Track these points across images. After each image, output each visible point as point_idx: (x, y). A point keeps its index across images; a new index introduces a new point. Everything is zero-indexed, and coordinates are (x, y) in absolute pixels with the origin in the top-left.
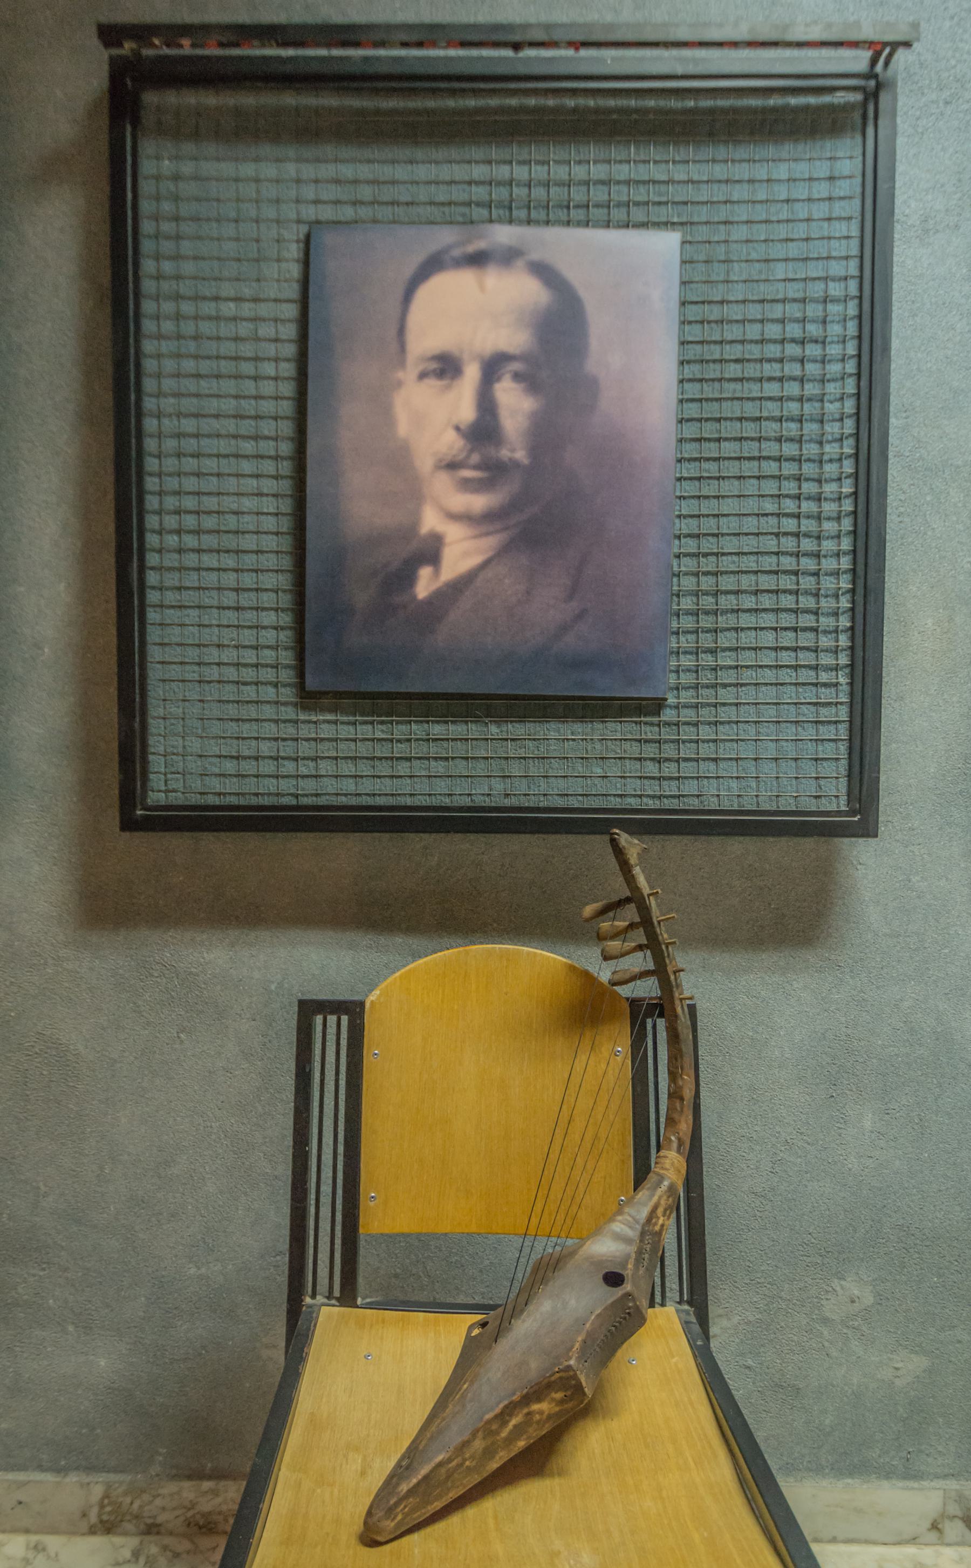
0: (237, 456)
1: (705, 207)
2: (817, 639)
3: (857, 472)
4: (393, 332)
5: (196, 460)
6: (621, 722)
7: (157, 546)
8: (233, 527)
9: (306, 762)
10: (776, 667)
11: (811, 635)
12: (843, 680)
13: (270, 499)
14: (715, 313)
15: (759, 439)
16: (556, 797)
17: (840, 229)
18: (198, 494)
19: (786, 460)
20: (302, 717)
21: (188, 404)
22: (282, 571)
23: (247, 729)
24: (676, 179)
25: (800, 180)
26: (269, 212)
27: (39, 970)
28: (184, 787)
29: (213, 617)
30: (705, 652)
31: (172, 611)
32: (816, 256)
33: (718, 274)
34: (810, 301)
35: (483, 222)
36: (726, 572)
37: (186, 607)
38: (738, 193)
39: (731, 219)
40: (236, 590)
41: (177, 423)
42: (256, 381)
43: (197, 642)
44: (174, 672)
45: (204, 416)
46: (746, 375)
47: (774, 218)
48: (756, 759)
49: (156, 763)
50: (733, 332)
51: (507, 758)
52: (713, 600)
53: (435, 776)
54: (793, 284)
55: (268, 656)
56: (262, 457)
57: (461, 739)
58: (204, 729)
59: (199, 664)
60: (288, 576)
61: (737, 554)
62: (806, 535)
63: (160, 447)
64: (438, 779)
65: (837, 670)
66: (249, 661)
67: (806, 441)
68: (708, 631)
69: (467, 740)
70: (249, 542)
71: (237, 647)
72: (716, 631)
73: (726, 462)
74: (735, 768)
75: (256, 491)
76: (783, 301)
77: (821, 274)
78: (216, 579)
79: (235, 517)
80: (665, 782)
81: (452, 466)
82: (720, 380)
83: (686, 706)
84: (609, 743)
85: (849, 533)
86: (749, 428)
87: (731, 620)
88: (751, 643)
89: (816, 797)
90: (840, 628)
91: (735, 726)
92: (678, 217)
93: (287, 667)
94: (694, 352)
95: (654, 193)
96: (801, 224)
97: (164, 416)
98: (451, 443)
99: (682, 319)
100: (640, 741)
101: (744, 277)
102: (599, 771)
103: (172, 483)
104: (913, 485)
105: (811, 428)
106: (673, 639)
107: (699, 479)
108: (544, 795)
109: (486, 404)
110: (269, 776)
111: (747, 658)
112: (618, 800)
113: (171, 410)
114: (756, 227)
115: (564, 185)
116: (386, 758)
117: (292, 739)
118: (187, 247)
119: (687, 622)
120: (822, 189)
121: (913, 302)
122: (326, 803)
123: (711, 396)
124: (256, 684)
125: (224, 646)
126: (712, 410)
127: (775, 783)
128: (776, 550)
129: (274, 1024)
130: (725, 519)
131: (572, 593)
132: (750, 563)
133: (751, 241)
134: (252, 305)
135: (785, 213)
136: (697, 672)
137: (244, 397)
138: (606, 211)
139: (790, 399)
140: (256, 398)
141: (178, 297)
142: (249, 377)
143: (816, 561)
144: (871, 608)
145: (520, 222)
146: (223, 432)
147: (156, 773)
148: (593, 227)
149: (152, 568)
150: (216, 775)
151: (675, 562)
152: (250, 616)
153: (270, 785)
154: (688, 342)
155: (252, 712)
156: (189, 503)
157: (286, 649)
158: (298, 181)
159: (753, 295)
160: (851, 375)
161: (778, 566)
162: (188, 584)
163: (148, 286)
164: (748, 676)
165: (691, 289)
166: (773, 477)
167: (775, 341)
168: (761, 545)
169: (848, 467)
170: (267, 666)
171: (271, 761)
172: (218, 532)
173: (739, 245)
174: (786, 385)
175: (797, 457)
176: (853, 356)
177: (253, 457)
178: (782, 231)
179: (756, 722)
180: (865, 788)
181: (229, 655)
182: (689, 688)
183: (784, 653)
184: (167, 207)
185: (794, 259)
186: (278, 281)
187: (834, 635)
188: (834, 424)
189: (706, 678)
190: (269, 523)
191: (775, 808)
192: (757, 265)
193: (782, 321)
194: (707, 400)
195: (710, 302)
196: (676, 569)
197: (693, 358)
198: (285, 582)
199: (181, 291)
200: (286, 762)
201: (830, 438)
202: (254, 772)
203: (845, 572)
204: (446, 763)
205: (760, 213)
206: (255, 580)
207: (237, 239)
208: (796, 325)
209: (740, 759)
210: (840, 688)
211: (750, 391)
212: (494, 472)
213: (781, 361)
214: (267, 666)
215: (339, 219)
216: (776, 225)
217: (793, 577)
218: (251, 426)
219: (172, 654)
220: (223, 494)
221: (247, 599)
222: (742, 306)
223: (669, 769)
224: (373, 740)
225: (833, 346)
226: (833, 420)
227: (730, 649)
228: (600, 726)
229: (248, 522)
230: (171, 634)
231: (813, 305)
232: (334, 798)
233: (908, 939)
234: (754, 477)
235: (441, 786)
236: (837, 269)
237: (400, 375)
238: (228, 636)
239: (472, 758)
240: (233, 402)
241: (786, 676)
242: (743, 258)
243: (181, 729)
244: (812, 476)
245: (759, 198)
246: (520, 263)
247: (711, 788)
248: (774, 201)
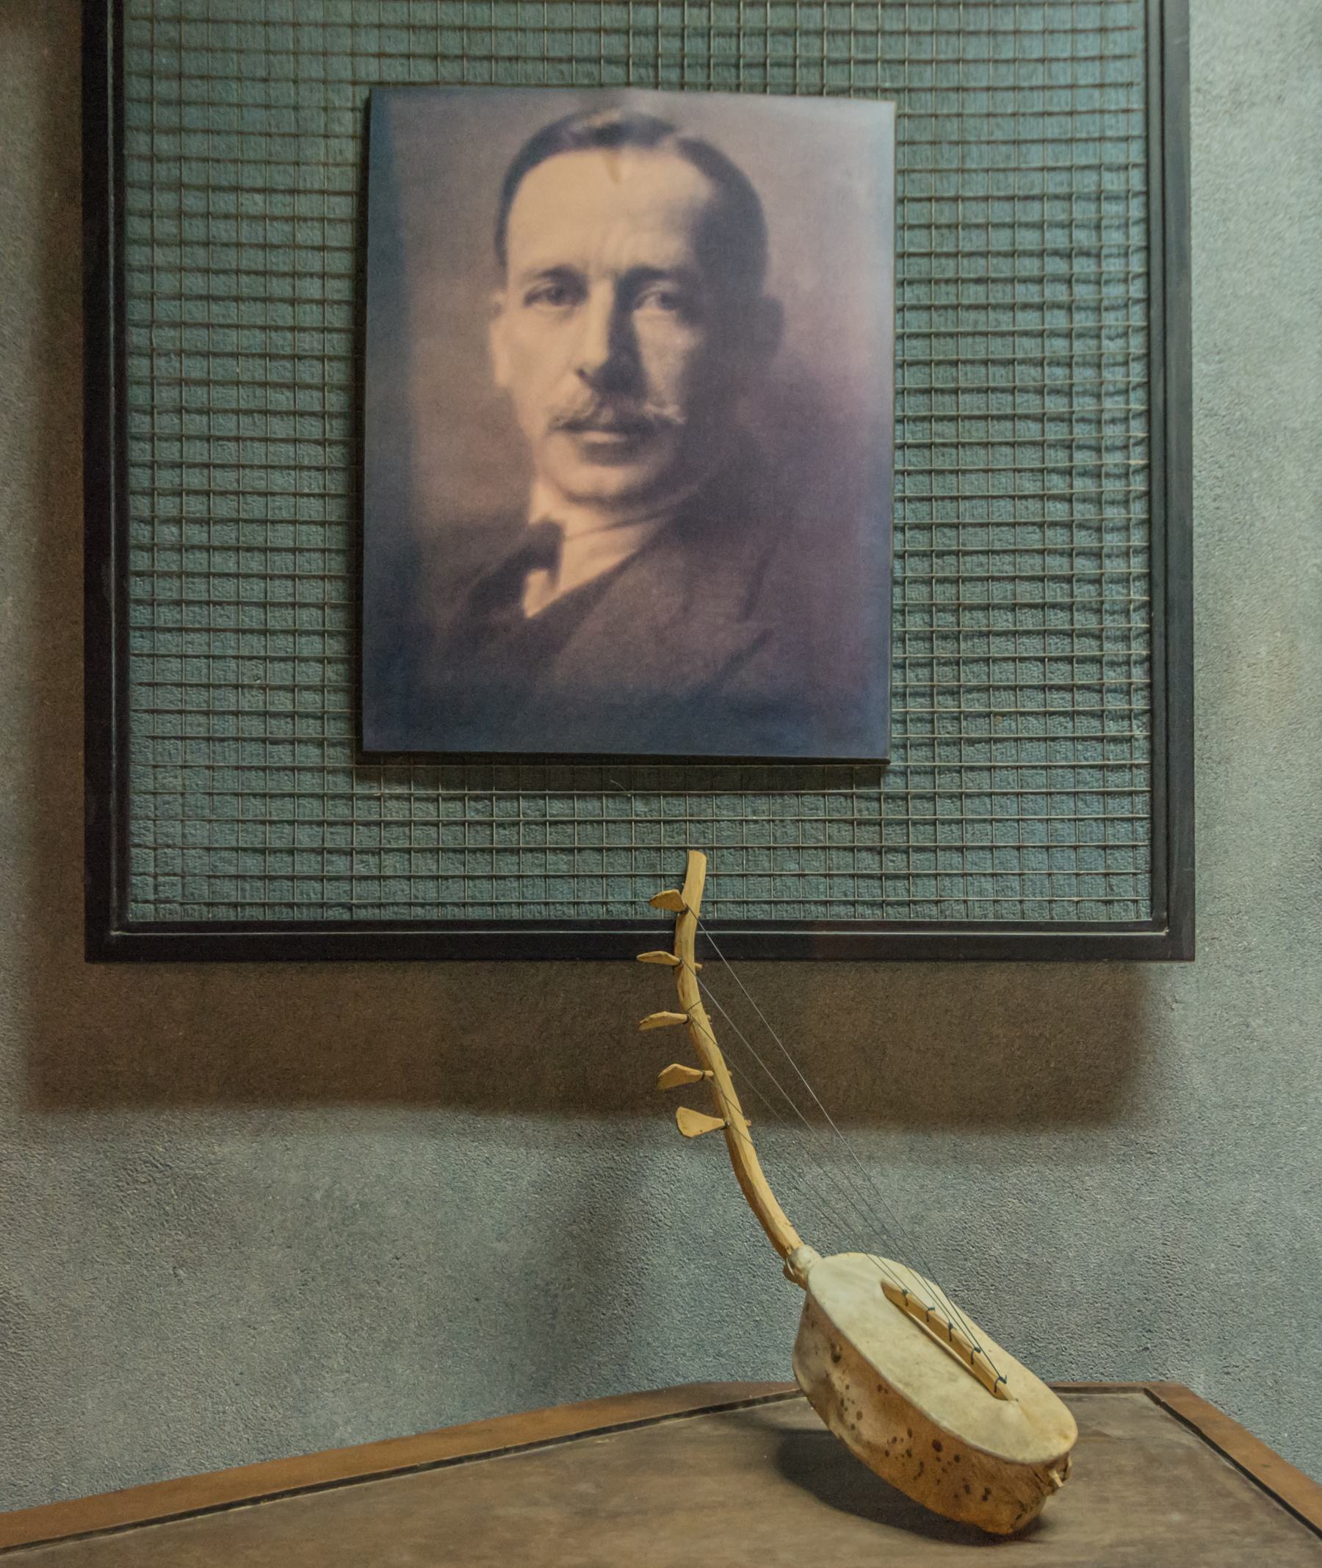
0: (265, 412)
1: (929, 68)
2: (1102, 673)
3: (1149, 438)
4: (488, 235)
5: (205, 418)
6: (824, 795)
7: (146, 541)
8: (258, 514)
9: (365, 857)
10: (1045, 714)
11: (1093, 668)
12: (1139, 732)
13: (313, 473)
14: (944, 214)
15: (1012, 391)
17: (1117, 99)
18: (207, 466)
19: (1051, 420)
20: (359, 790)
21: (196, 338)
22: (330, 578)
23: (278, 809)
24: (887, 28)
25: (1059, 32)
26: (313, 69)
28: (184, 895)
29: (229, 644)
30: (943, 694)
31: (168, 636)
32: (1084, 135)
33: (949, 161)
34: (1078, 198)
35: (617, 85)
36: (971, 579)
37: (187, 630)
38: (974, 49)
39: (965, 84)
40: (263, 605)
41: (178, 365)
42: (293, 305)
43: (205, 681)
44: (169, 725)
45: (216, 355)
46: (992, 301)
47: (1025, 84)
48: (1018, 848)
49: (142, 859)
50: (974, 241)
51: (658, 849)
52: (953, 619)
53: (554, 877)
54: (1052, 174)
55: (310, 701)
56: (302, 414)
57: (592, 822)
58: (213, 810)
59: (206, 713)
60: (340, 585)
61: (986, 553)
62: (1082, 526)
63: (153, 399)
65: (1130, 719)
66: (281, 708)
67: (1077, 393)
68: (947, 663)
69: (600, 822)
70: (282, 536)
71: (263, 688)
72: (958, 664)
73: (967, 423)
74: (989, 862)
75: (292, 463)
76: (1040, 198)
77: (1093, 161)
78: (233, 588)
79: (262, 500)
80: (890, 883)
81: (574, 426)
82: (956, 307)
83: (917, 772)
84: (808, 826)
85: (1142, 522)
86: (998, 376)
87: (980, 648)
88: (1008, 679)
90: (1133, 658)
91: (987, 800)
92: (892, 81)
93: (336, 717)
94: (917, 268)
95: (857, 48)
96: (1062, 92)
97: (159, 355)
98: (570, 393)
99: (900, 221)
100: (851, 823)
101: (985, 166)
102: (793, 867)
103: (169, 451)
104: (1233, 455)
105: (1083, 376)
106: (897, 674)
107: (929, 446)
108: (714, 903)
109: (622, 338)
111: (1004, 702)
112: (822, 909)
113: (170, 346)
114: (1000, 96)
115: (731, 35)
116: (483, 850)
117: (344, 823)
118: (193, 116)
119: (917, 651)
120: (1089, 46)
121: (1224, 201)
122: (394, 917)
123: (943, 329)
124: (292, 743)
125: (243, 687)
126: (945, 349)
127: (1046, 882)
128: (1038, 546)
130: (967, 503)
131: (748, 608)
132: (1003, 566)
133: (995, 115)
134: (288, 199)
135: (1041, 77)
136: (932, 721)
137: (277, 329)
138: (789, 71)
139: (1054, 334)
140: (292, 329)
141: (180, 186)
142: (282, 300)
143: (1096, 563)
144: (1175, 628)
145: (670, 86)
146: (244, 378)
147: (141, 874)
148: (773, 93)
149: (139, 574)
150: (230, 877)
151: (897, 565)
152: (282, 644)
153: (312, 891)
154: (911, 255)
155: (285, 783)
156: (195, 479)
157: (336, 690)
158: (353, 26)
159: (998, 189)
160: (1137, 301)
161: (1043, 569)
162: (192, 597)
163: (137, 170)
164: (1004, 728)
165: (913, 181)
166: (1033, 444)
167: (1031, 254)
168: (1019, 540)
169: (1138, 430)
170: (307, 716)
171: (312, 857)
172: (237, 521)
173: (978, 121)
174: (1048, 315)
175: (1067, 416)
176: (1139, 276)
177: (288, 413)
178: (1038, 102)
179: (1017, 794)
180: (1174, 888)
181: (251, 701)
182: (920, 745)
183: (1055, 695)
184: (164, 60)
185: (1053, 141)
186: (325, 165)
187: (1125, 668)
188: (1117, 369)
189: (946, 730)
190: (313, 508)
192: (1003, 148)
193: (1039, 226)
194: (937, 335)
195: (938, 199)
196: (898, 574)
197: (917, 276)
198: (334, 594)
199: (185, 180)
200: (334, 858)
201: (1111, 389)
202: (287, 871)
203: (1138, 578)
204: (571, 858)
205: (1007, 76)
206: (290, 590)
207: (267, 107)
208: (1059, 232)
209: (997, 847)
210: (1136, 744)
211: (998, 322)
212: (634, 435)
213: (1040, 281)
214: (307, 716)
215: (412, 79)
216: (1027, 93)
217: (1065, 586)
218: (285, 368)
219: (165, 699)
220: (244, 467)
221: (278, 619)
222: (983, 205)
223: (894, 863)
224: (463, 824)
225: (1112, 260)
226: (1115, 365)
227: (978, 689)
228: (794, 801)
229: (282, 508)
230: (167, 670)
231: (1083, 204)
232: (404, 910)
233: (1249, 1112)
234: (1007, 444)
235: (562, 892)
236: (1114, 154)
237: (499, 297)
238: (250, 672)
239: (609, 849)
240: (260, 336)
241: (1061, 728)
242: (983, 138)
243: (179, 810)
244: (1088, 443)
245: (1003, 56)
246: (668, 142)
247: (955, 890)
248: (1024, 60)
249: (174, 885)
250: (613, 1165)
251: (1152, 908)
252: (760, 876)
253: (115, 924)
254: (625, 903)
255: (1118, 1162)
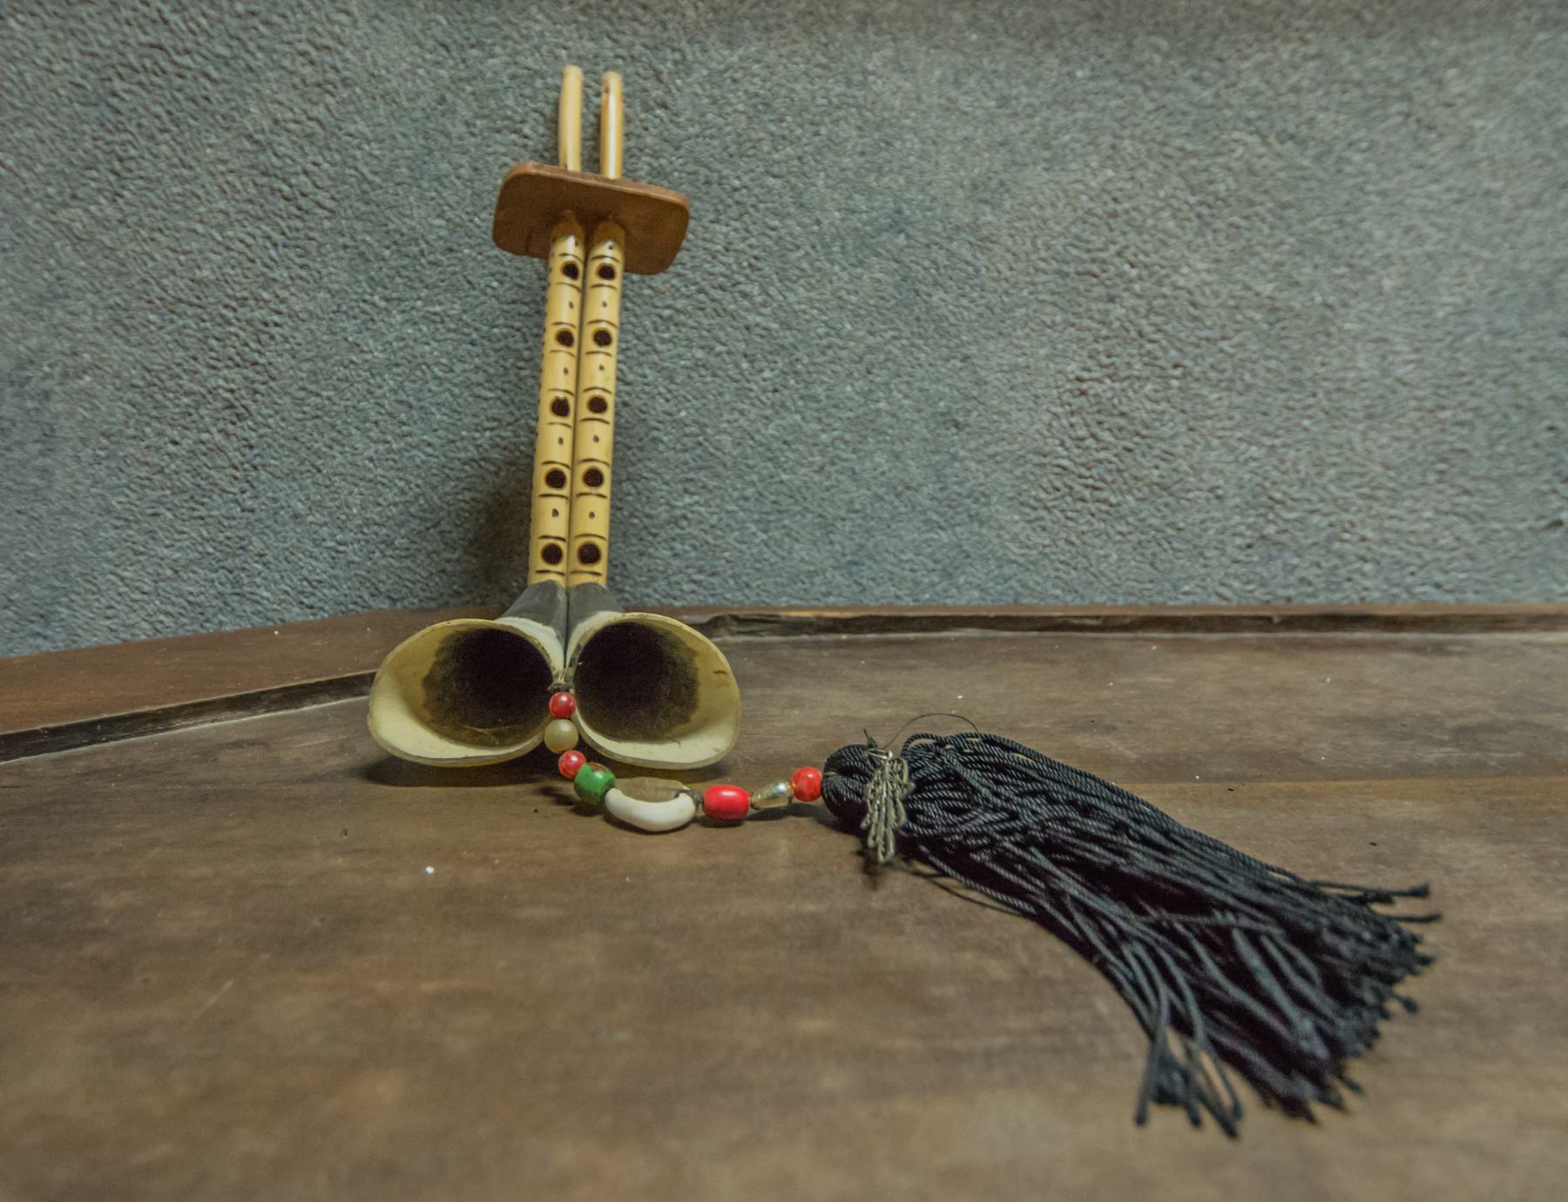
250: (166, 39)
255: (1542, 25)
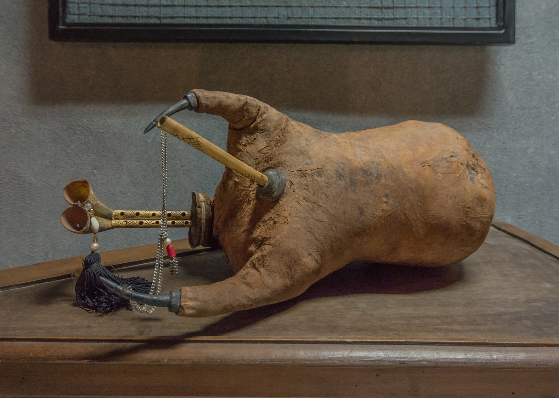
16: (319, 20)
27: (6, 130)
28: (90, 12)
53: (245, 6)
64: (247, 8)
89: (478, 19)
108: (312, 18)
110: (143, 5)
112: (357, 21)
122: (178, 22)
127: (451, 10)
129: (151, 164)
180: (507, 13)
191: (452, 26)
249: (85, 7)
251: (497, 21)
252: (331, 7)
253: (61, 23)
254: (274, 18)
